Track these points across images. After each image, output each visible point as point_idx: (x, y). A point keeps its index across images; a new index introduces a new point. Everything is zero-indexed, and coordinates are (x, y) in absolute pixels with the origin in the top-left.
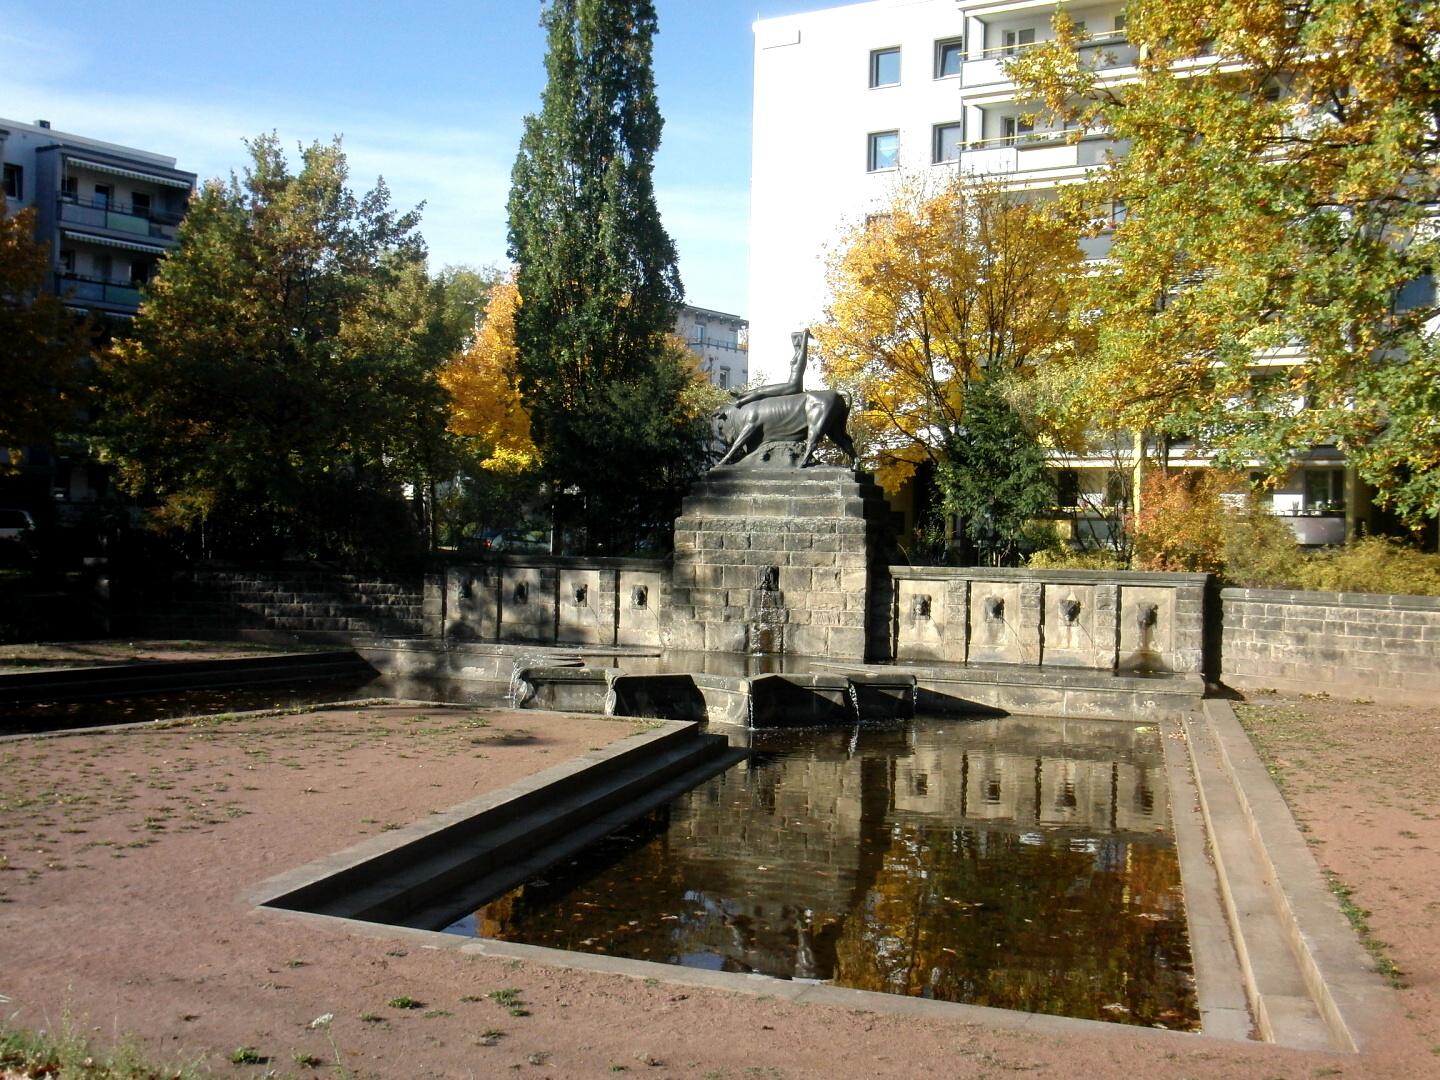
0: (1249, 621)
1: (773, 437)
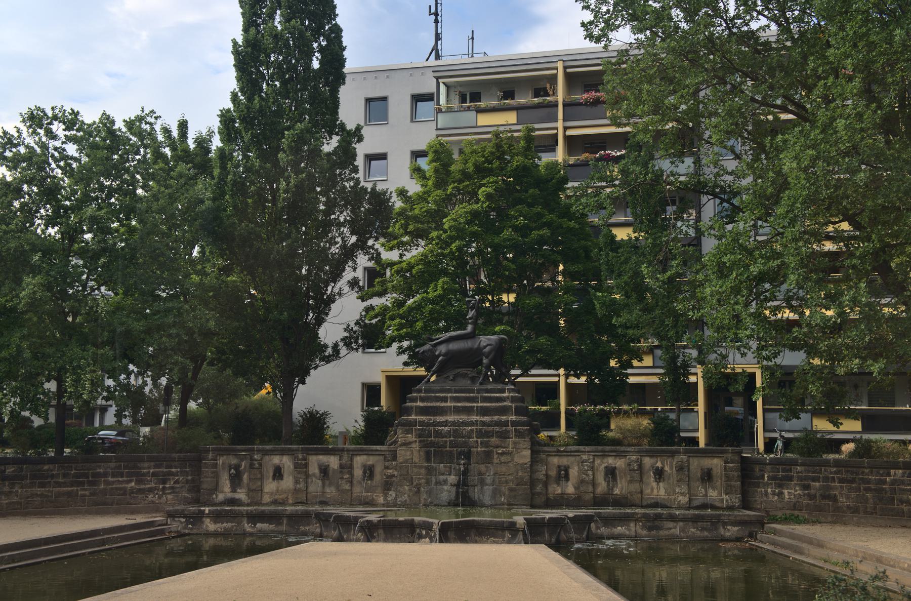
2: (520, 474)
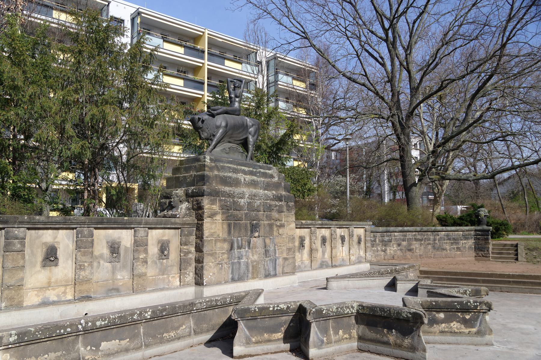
0: (379, 240)
1: (230, 140)
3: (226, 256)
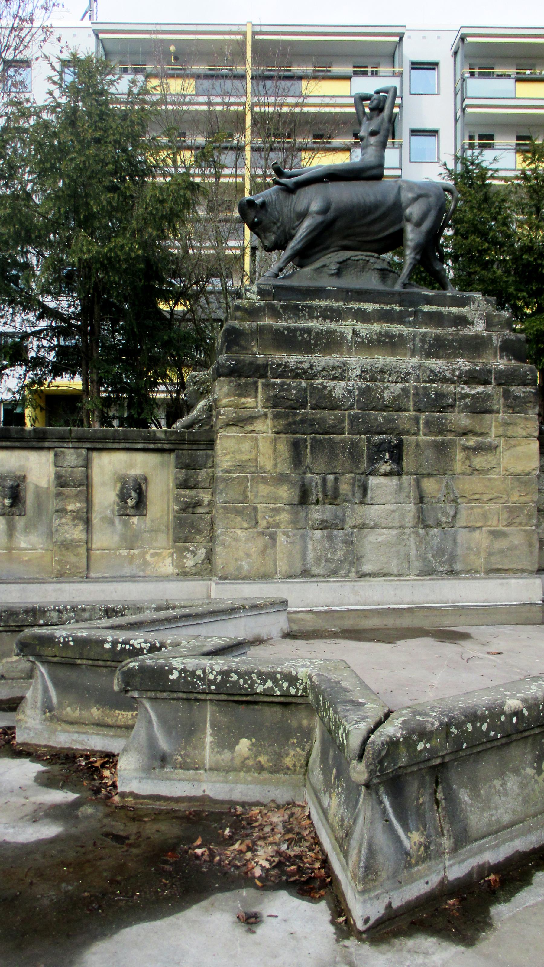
1: (346, 243)
2: (515, 497)
3: (284, 517)
